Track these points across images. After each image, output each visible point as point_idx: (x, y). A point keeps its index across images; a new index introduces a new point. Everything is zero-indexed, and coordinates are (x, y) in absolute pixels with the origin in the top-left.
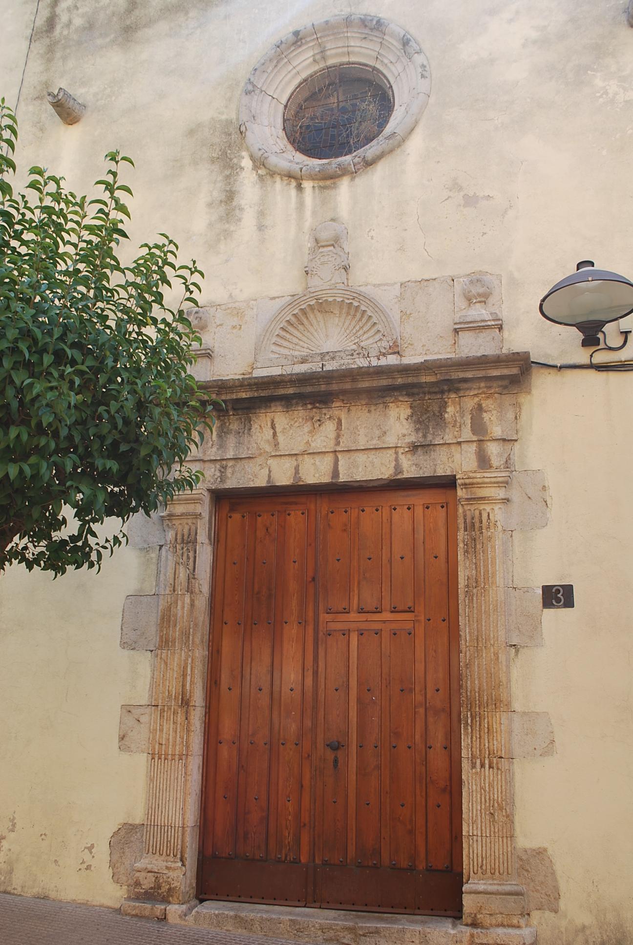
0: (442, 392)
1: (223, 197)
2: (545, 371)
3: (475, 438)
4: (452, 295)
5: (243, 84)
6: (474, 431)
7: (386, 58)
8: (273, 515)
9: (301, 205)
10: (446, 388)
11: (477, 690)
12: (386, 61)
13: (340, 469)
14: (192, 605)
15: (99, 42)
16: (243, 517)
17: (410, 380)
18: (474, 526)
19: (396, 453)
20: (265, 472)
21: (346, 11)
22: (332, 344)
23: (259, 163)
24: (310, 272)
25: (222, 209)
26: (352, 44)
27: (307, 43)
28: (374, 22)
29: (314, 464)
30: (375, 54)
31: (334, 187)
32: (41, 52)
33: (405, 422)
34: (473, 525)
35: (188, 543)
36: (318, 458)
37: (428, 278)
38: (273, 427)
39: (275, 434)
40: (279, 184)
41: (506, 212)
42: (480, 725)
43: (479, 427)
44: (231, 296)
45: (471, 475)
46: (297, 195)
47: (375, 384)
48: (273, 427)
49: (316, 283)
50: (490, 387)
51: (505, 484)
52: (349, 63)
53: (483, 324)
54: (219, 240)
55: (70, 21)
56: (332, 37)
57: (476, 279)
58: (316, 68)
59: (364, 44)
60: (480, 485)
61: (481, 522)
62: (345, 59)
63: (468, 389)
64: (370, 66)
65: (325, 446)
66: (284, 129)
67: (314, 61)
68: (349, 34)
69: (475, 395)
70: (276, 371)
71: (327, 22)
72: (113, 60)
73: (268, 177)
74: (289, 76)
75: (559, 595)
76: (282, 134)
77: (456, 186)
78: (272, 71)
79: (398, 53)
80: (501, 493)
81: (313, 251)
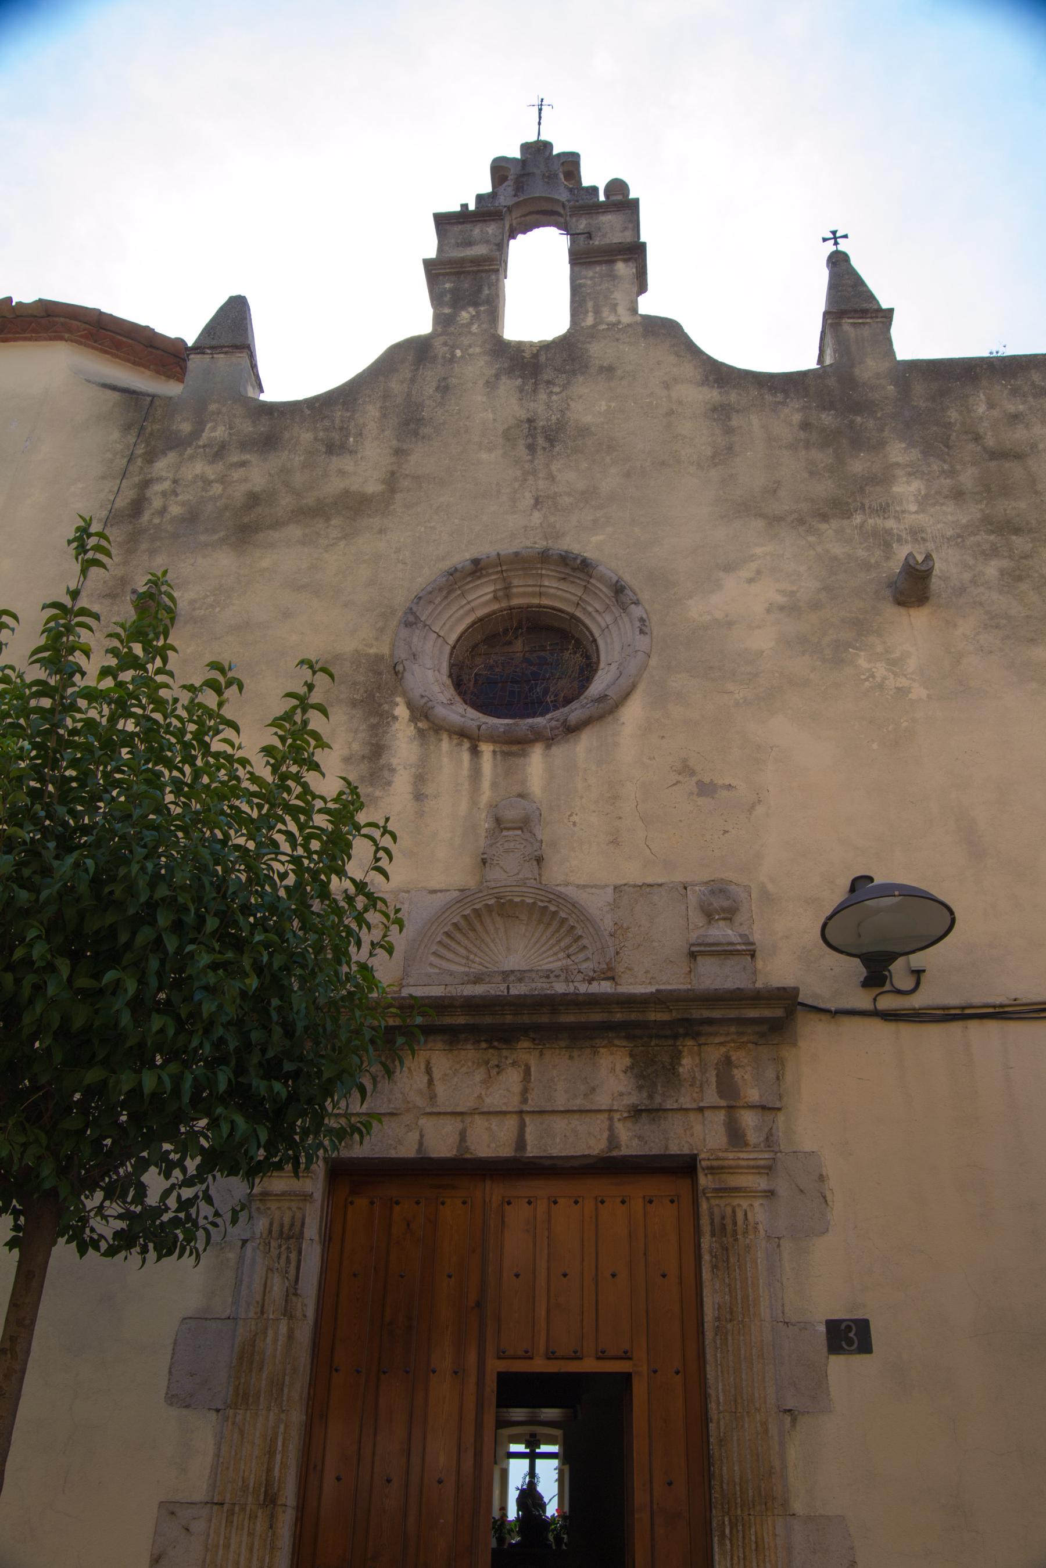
0: (676, 1037)
1: (366, 751)
2: (814, 1016)
3: (723, 1103)
4: (683, 908)
5: (400, 614)
6: (721, 1094)
8: (418, 1203)
9: (476, 774)
10: (681, 1030)
11: (737, 1480)
12: (590, 609)
13: (529, 1138)
14: (290, 1336)
15: (203, 538)
16: (372, 1203)
17: (634, 1016)
18: (726, 1229)
19: (611, 1119)
20: (414, 1136)
21: (541, 544)
22: (521, 960)
23: (420, 713)
24: (489, 861)
26: (547, 584)
28: (579, 561)
29: (489, 1129)
30: (575, 599)
31: (524, 754)
32: (118, 539)
33: (622, 1075)
34: (723, 1227)
35: (289, 1238)
36: (494, 1122)
38: (429, 1071)
39: (431, 1082)
40: (445, 744)
41: (753, 807)
42: (744, 1537)
43: (728, 1089)
45: (721, 1154)
47: (583, 1018)
48: (429, 1071)
49: (496, 876)
50: (742, 1034)
51: (768, 1170)
52: (539, 606)
53: (730, 948)
55: (164, 510)
56: (520, 573)
57: (719, 889)
58: (496, 606)
59: (563, 585)
60: (732, 1170)
61: (735, 1224)
62: (535, 601)
63: (711, 1034)
64: (568, 613)
65: (505, 1104)
66: (450, 676)
67: (496, 598)
68: (544, 572)
69: (721, 1044)
70: (436, 991)
71: (517, 554)
72: (223, 562)
73: (431, 733)
74: (462, 612)
75: (851, 1335)
76: (449, 682)
77: (686, 769)
78: (440, 603)
79: (607, 601)
80: (762, 1183)
81: (491, 834)
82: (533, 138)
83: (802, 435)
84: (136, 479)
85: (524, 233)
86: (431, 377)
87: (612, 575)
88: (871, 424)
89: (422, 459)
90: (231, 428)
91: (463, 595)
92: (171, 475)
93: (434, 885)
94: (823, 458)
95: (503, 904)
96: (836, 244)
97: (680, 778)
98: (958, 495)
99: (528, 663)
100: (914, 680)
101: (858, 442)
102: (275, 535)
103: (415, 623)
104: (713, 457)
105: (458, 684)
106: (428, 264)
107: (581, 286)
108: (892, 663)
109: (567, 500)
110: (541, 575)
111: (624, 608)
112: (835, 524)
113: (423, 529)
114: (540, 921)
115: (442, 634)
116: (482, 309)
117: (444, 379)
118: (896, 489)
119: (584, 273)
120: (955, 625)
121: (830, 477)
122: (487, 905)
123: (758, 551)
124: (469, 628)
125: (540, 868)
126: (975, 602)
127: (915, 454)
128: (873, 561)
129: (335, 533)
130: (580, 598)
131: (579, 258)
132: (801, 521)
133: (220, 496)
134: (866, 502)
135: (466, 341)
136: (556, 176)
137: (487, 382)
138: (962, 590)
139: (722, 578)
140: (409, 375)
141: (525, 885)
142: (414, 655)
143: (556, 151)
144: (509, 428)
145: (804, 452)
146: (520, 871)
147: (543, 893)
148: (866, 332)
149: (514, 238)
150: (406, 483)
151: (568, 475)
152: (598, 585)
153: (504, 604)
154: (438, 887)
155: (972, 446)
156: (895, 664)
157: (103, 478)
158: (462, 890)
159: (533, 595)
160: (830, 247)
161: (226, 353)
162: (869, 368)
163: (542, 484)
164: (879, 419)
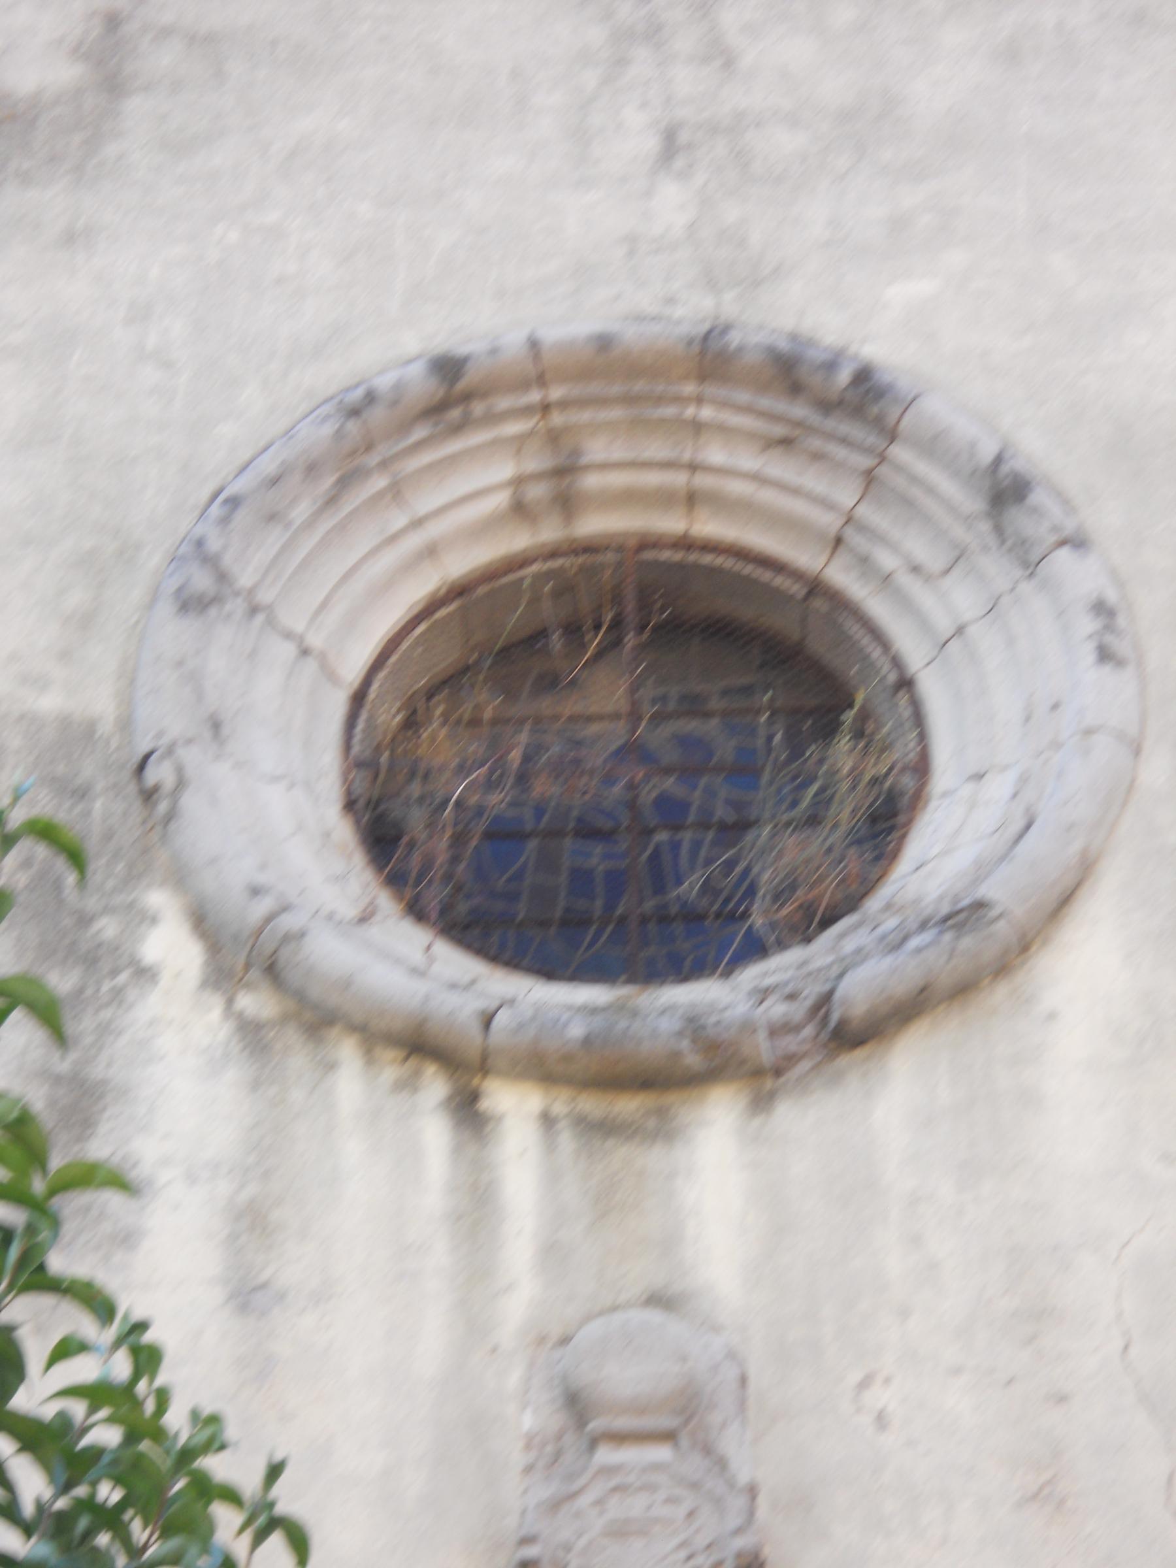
5: (153, 560)
7: (894, 547)
9: (476, 1207)
12: (886, 560)
21: (694, 310)
23: (249, 955)
27: (492, 418)
28: (844, 376)
30: (830, 521)
31: (661, 1130)
40: (351, 1080)
46: (457, 1150)
52: (685, 543)
56: (616, 413)
58: (518, 541)
59: (779, 467)
62: (671, 523)
64: (797, 575)
66: (350, 805)
67: (520, 510)
68: (707, 413)
71: (604, 343)
73: (292, 1035)
74: (390, 558)
78: (310, 523)
81: (547, 1456)
91: (396, 492)
105: (381, 838)
109: (783, 143)
110: (697, 427)
111: (1030, 563)
113: (233, 236)
115: (315, 640)
150: (164, 59)
152: (922, 467)
153: (549, 532)
159: (663, 499)
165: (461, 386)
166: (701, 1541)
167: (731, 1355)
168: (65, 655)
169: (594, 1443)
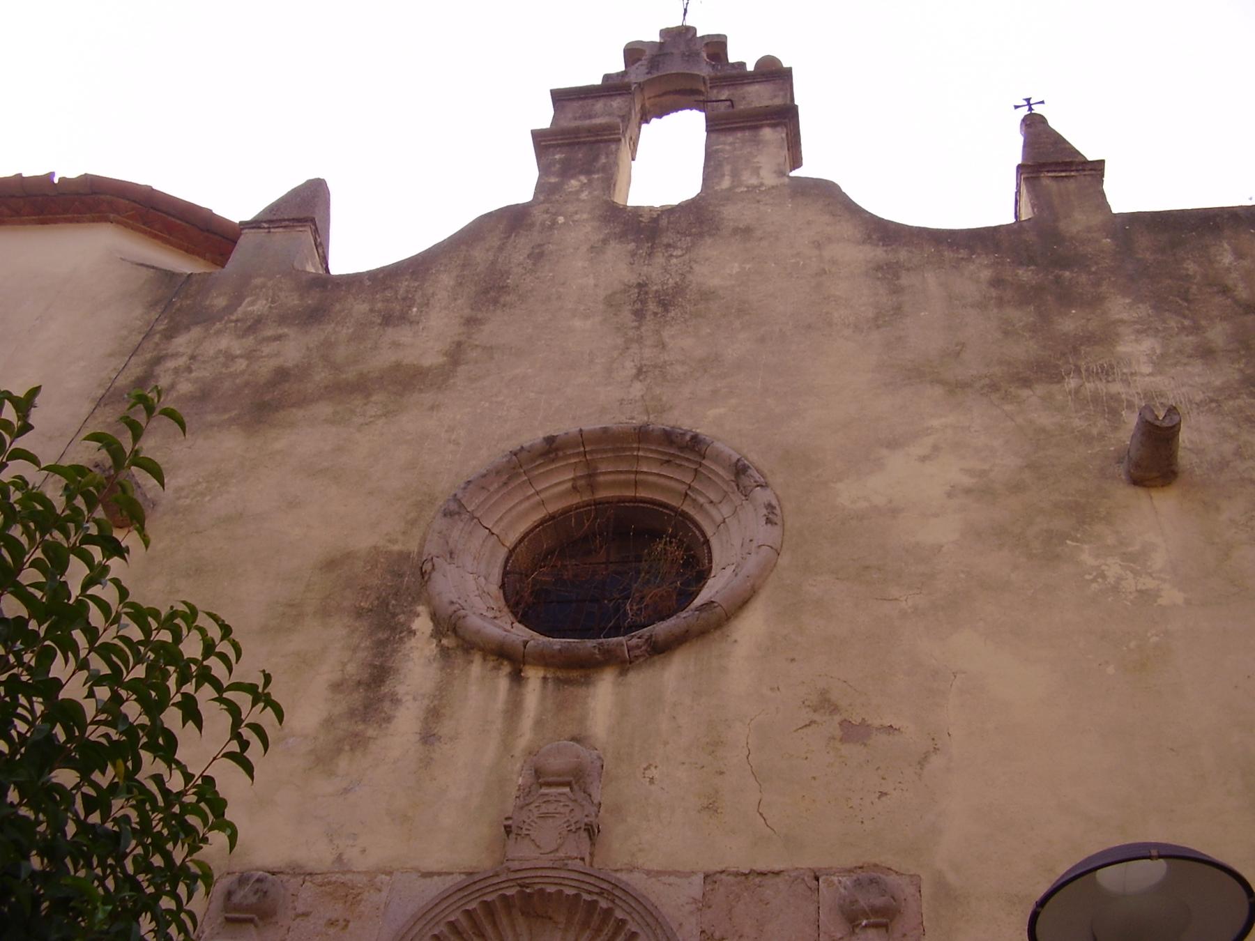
4: (812, 908)
7: (701, 493)
9: (514, 708)
12: (701, 500)
15: (210, 418)
21: (639, 419)
23: (448, 627)
24: (514, 828)
25: (357, 697)
26: (645, 470)
28: (688, 438)
31: (587, 682)
37: (761, 866)
40: (477, 667)
41: (923, 761)
44: (339, 858)
46: (510, 689)
49: (523, 853)
52: (635, 500)
54: (339, 751)
57: (869, 877)
58: (575, 500)
62: (630, 493)
64: (672, 509)
66: (502, 586)
67: (574, 488)
68: (641, 453)
72: (229, 444)
73: (459, 653)
74: (526, 504)
77: (826, 704)
78: (497, 491)
79: (725, 487)
81: (526, 793)
82: (675, 22)
83: (994, 293)
84: (148, 356)
85: (660, 116)
86: (522, 246)
87: (732, 452)
88: (1083, 278)
89: (499, 328)
90: (273, 302)
92: (189, 352)
93: (430, 864)
94: (1021, 316)
95: (530, 894)
96: (1030, 109)
97: (816, 717)
98: (1206, 353)
99: (611, 565)
100: (1164, 581)
101: (1067, 298)
102: (299, 413)
103: (459, 513)
104: (876, 318)
106: (539, 138)
107: (717, 151)
108: (1129, 558)
109: (680, 369)
110: (638, 458)
112: (1040, 389)
114: (585, 925)
115: (495, 531)
116: (596, 176)
117: (540, 246)
118: (1121, 349)
119: (722, 138)
120: (1218, 509)
121: (1032, 338)
122: (504, 897)
123: (935, 423)
124: (536, 527)
125: (593, 844)
126: (1242, 479)
127: (1144, 310)
128: (1095, 431)
129: (372, 410)
130: (690, 487)
131: (714, 127)
132: (994, 387)
133: (243, 373)
134: (1083, 364)
135: (571, 208)
136: (698, 54)
137: (592, 247)
138: (1223, 465)
139: (893, 469)
140: (497, 243)
141: (564, 867)
142: (451, 553)
143: (699, 34)
144: (615, 293)
145: (995, 310)
146: (562, 845)
147: (592, 880)
148: (1071, 185)
149: (647, 122)
151: (682, 341)
154: (435, 867)
155: (1219, 299)
156: (1135, 560)
157: (111, 355)
158: (471, 874)
159: (625, 484)
160: (1024, 111)
161: (285, 227)
162: (1077, 222)
163: (647, 352)
164: (1094, 273)
165: (554, 445)
166: (573, 821)
167: (599, 758)
168: (404, 533)
169: (541, 785)
